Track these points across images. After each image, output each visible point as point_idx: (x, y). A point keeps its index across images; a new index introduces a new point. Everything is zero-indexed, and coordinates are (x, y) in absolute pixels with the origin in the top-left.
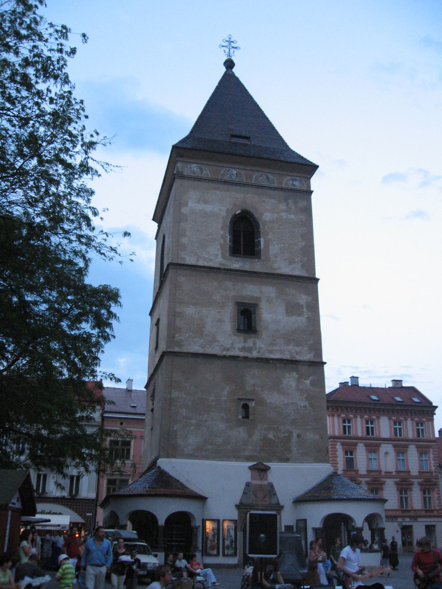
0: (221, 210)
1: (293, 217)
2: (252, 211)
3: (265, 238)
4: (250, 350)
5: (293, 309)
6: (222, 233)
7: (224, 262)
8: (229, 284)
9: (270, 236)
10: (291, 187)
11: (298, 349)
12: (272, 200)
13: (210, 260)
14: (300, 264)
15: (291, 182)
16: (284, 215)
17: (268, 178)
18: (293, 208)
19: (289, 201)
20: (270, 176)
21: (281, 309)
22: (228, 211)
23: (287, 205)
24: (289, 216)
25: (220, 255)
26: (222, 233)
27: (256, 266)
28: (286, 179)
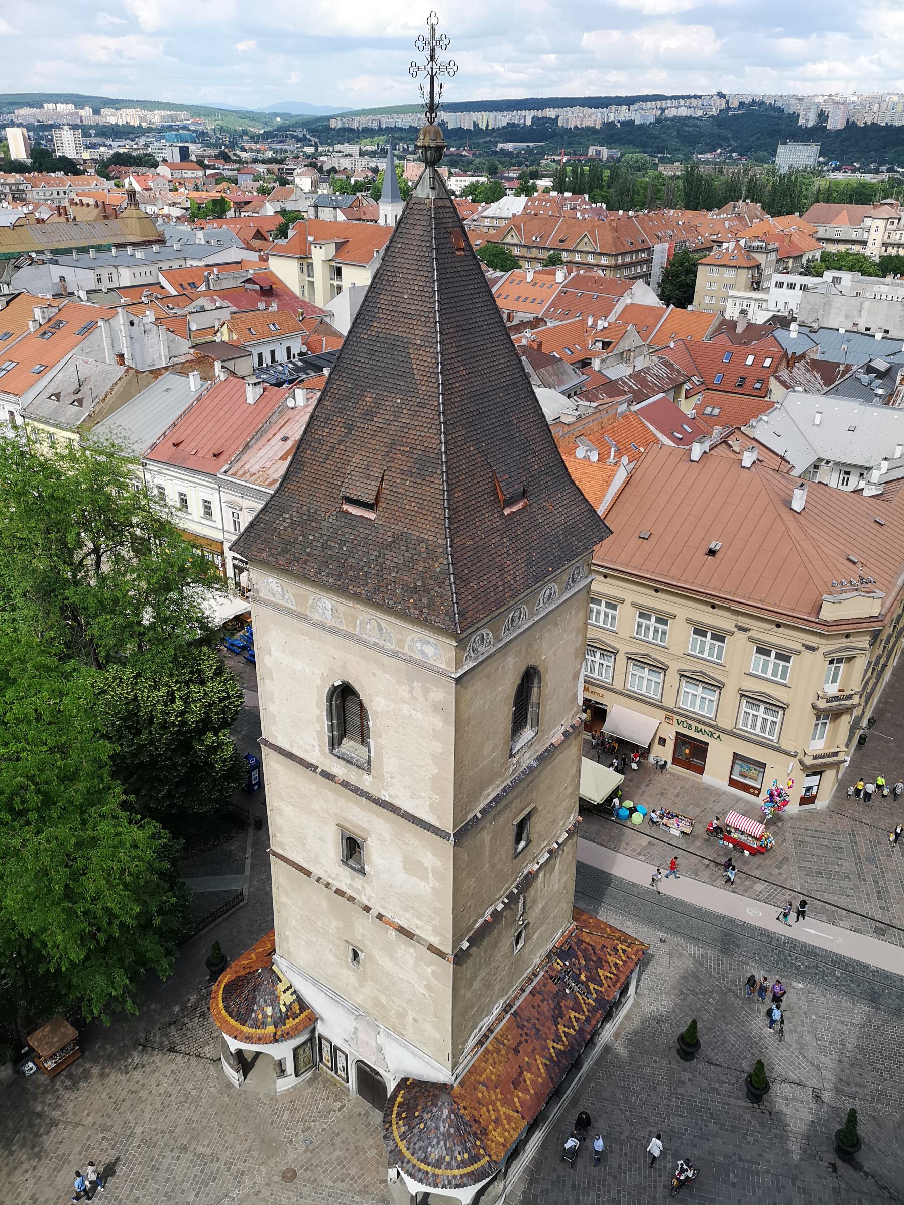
0: (313, 673)
1: (419, 716)
2: (357, 688)
3: (376, 742)
4: (358, 891)
5: (412, 866)
6: (318, 712)
7: (322, 759)
8: (330, 795)
9: (383, 741)
10: (417, 656)
11: (419, 923)
12: (388, 676)
13: (306, 751)
14: (428, 803)
15: (419, 645)
16: (406, 709)
17: (380, 629)
18: (421, 699)
19: (415, 684)
20: (383, 625)
21: (398, 860)
22: (322, 677)
23: (411, 692)
24: (413, 712)
25: (318, 748)
26: (318, 712)
27: (366, 782)
28: (410, 638)
